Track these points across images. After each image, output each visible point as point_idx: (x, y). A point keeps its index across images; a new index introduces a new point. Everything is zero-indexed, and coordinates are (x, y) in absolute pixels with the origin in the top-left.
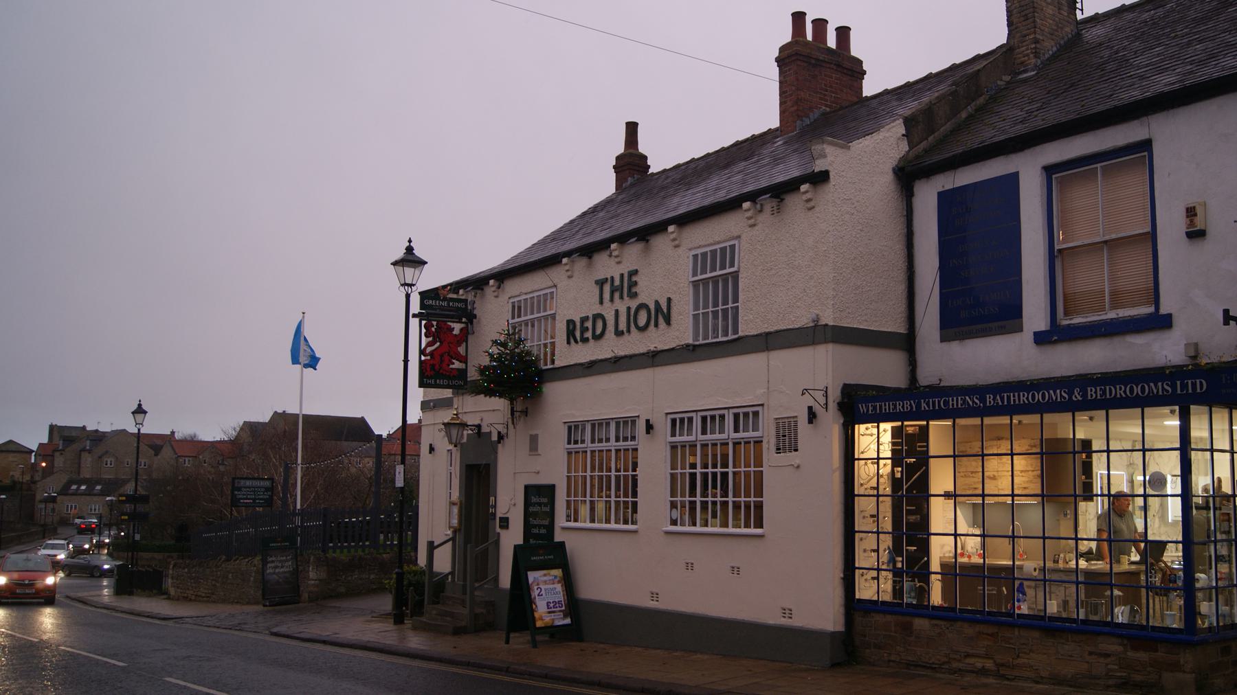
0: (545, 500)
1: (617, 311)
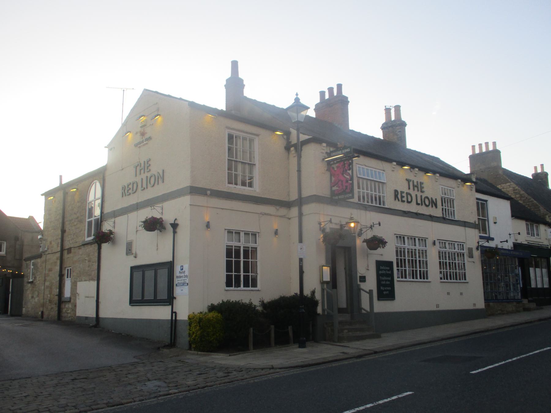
0: (388, 268)
1: (416, 195)
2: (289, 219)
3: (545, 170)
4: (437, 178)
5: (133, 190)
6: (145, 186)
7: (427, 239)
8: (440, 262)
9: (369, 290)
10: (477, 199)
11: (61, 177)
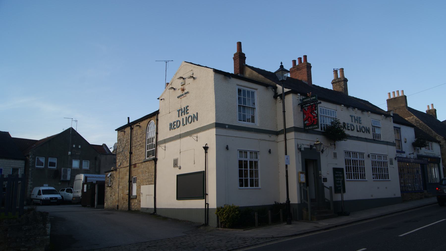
1: (357, 125)
2: (278, 142)
3: (434, 108)
4: (369, 114)
5: (177, 126)
6: (185, 123)
7: (364, 154)
8: (373, 168)
9: (330, 187)
10: (394, 127)
11: (129, 118)
